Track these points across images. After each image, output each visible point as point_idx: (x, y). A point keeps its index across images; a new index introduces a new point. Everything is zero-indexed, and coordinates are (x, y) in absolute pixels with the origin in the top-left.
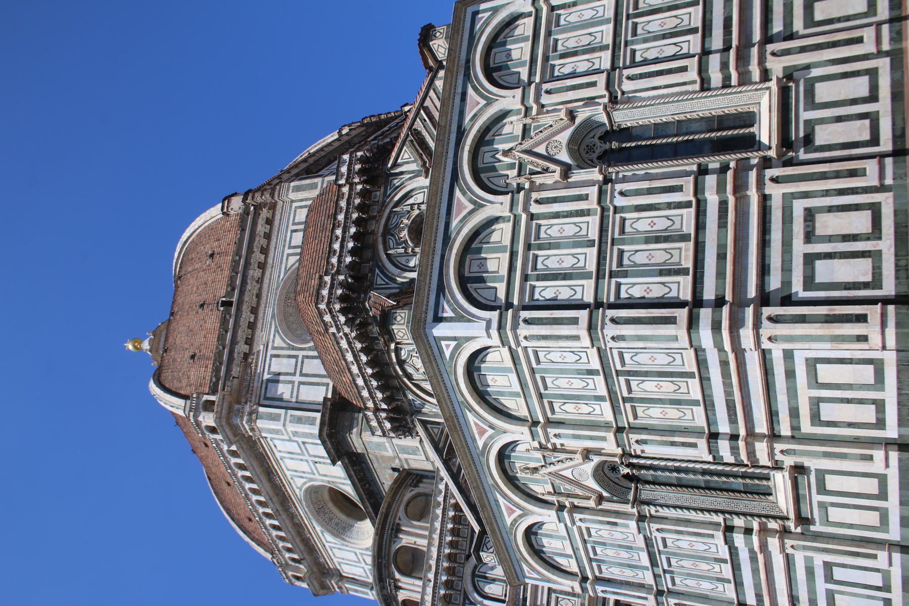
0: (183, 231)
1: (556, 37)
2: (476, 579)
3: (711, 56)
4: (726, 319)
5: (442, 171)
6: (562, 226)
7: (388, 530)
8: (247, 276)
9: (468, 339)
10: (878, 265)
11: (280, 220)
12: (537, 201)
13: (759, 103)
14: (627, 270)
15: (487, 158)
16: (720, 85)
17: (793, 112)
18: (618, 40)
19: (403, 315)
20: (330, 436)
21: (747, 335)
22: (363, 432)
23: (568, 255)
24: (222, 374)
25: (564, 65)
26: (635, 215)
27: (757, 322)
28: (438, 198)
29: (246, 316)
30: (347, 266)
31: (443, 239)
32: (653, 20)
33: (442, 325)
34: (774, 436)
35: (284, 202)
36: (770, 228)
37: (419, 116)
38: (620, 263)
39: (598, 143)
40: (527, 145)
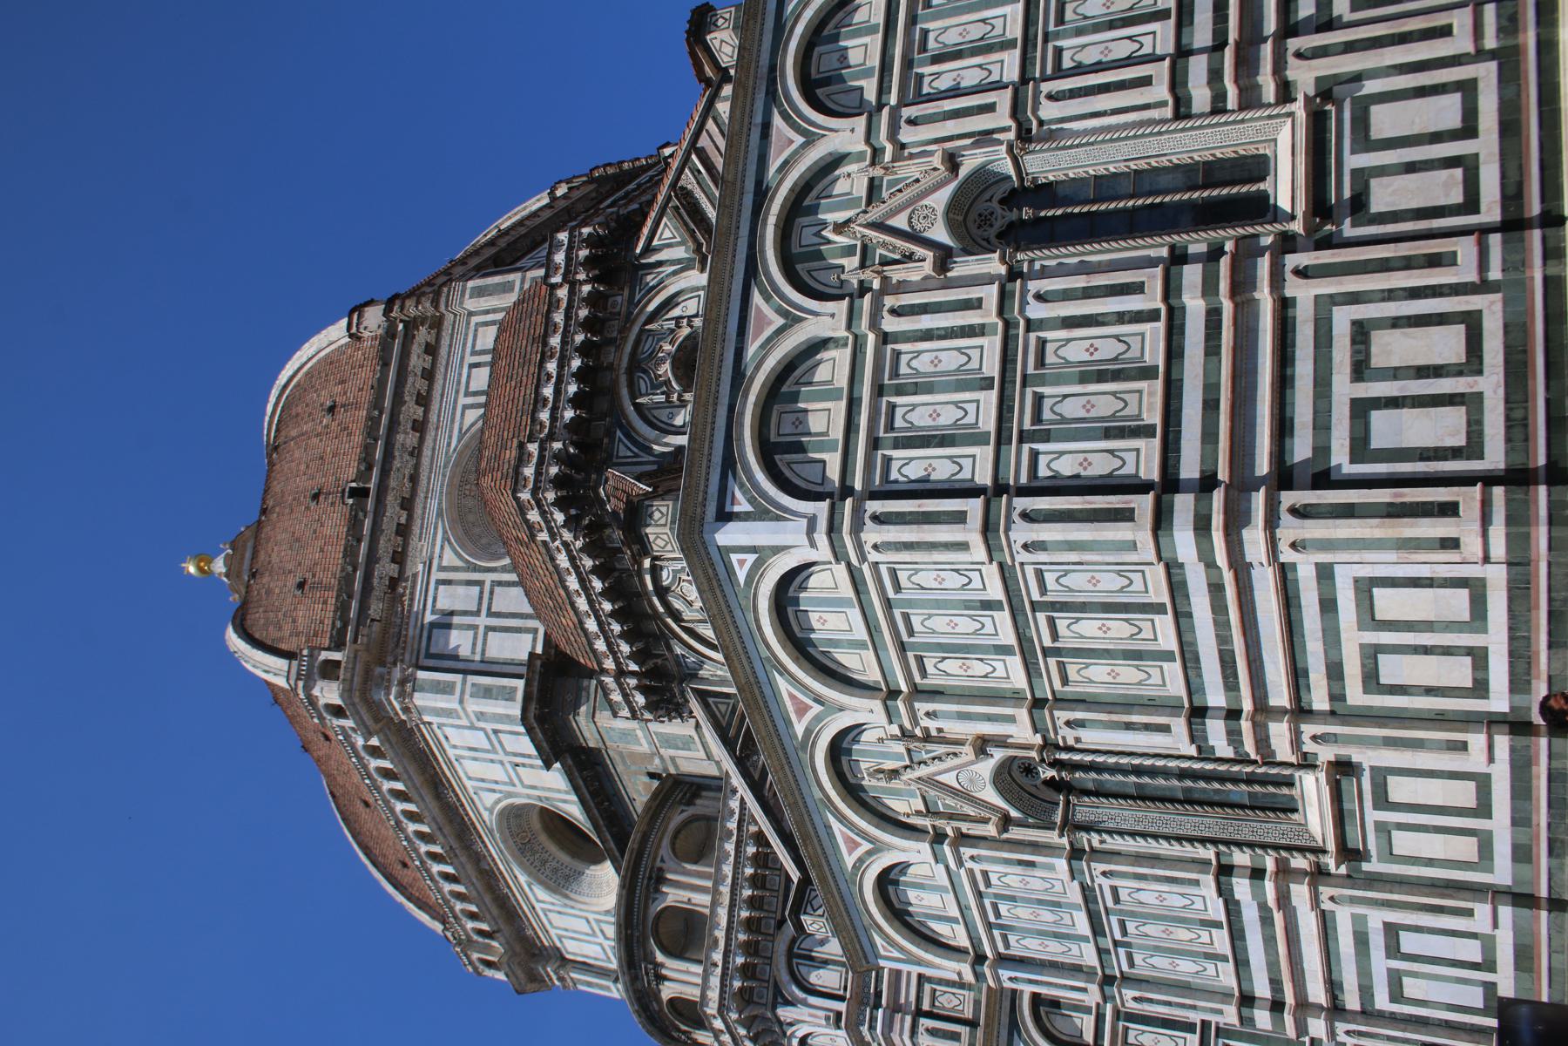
0: (282, 367)
1: (925, 26)
2: (795, 960)
3: (1192, 59)
4: (1219, 513)
5: (729, 260)
7: (643, 879)
8: (394, 445)
9: (777, 550)
11: (450, 346)
13: (1275, 140)
14: (1049, 430)
15: (808, 237)
16: (1208, 109)
17: (1333, 156)
19: (664, 510)
20: (541, 719)
21: (1254, 540)
22: (597, 712)
23: (947, 403)
25: (938, 74)
26: (1063, 334)
27: (1272, 516)
28: (723, 307)
29: (393, 513)
30: (566, 426)
31: (733, 378)
33: (731, 525)
34: (1300, 712)
35: (456, 315)
37: (690, 164)
38: (1037, 417)
40: (875, 213)
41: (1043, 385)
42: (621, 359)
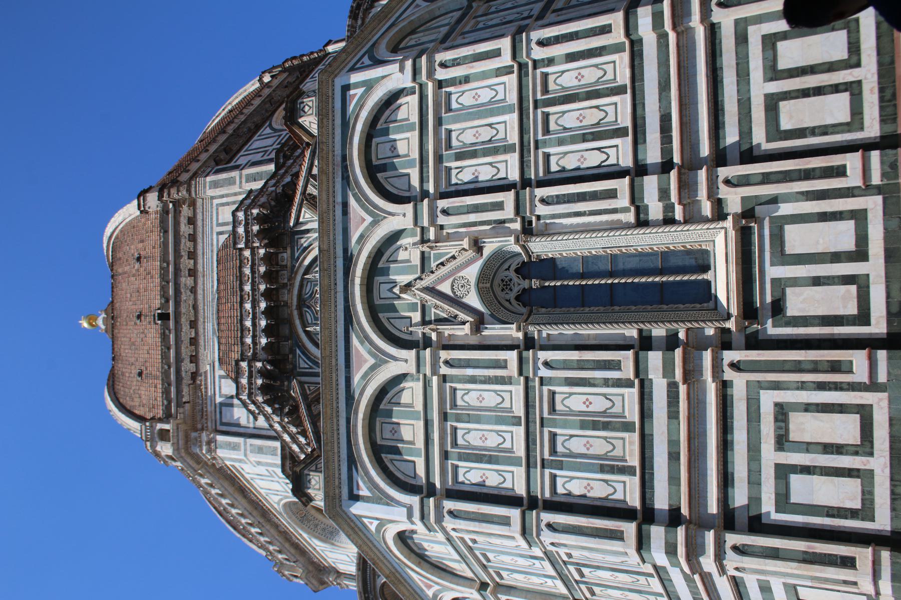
1: (449, 127)
4: (682, 545)
5: (333, 310)
6: (481, 392)
12: (447, 363)
14: (562, 461)
16: (661, 217)
17: (757, 267)
18: (526, 137)
21: (708, 563)
23: (491, 431)
25: (461, 168)
26: (566, 389)
27: (720, 551)
28: (333, 345)
30: (263, 349)
38: (553, 451)
39: (515, 280)
40: (428, 281)
41: (555, 427)
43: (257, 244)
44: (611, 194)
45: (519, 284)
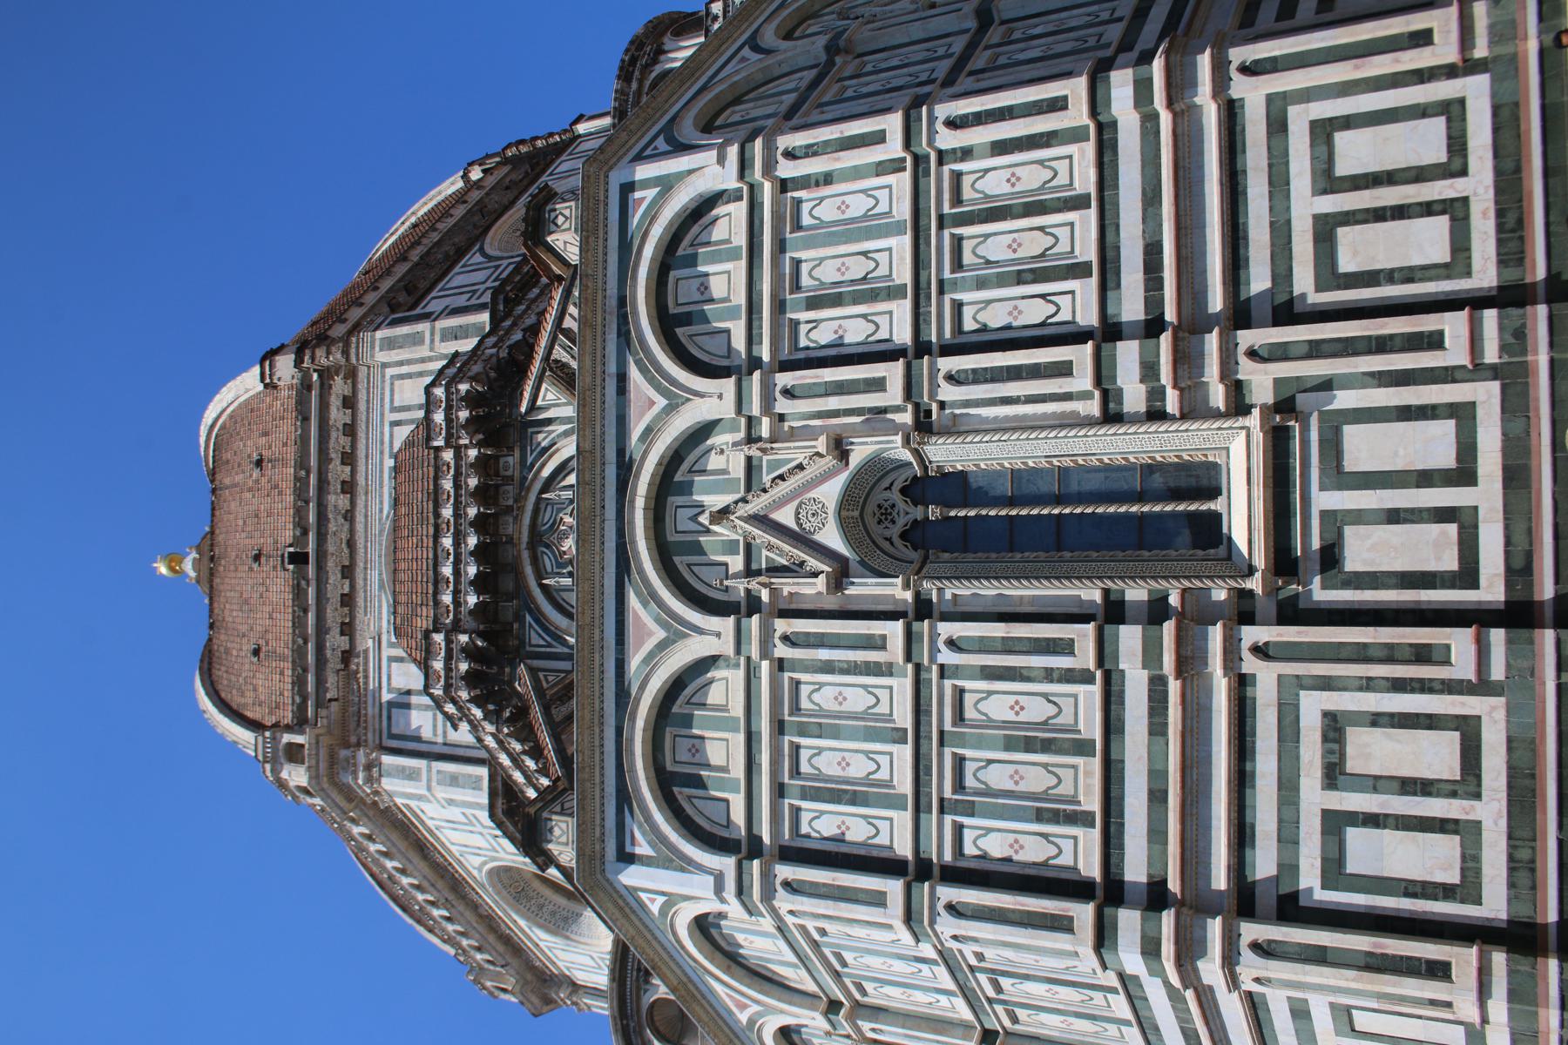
1: (796, 255)
3: (1121, 346)
4: (1169, 940)
5: (597, 549)
8: (326, 507)
10: (1473, 852)
11: (368, 401)
12: (786, 639)
14: (973, 802)
15: (683, 519)
16: (1143, 409)
17: (1298, 492)
19: (564, 826)
21: (1211, 970)
23: (857, 751)
24: (311, 687)
25: (816, 323)
27: (1230, 950)
28: (597, 607)
29: (336, 585)
30: (471, 612)
31: (617, 695)
32: (995, 234)
33: (633, 868)
35: (369, 367)
36: (1254, 748)
37: (559, 342)
38: (959, 786)
39: (901, 505)
40: (756, 505)
41: (963, 747)
42: (520, 533)
43: (465, 441)
44: (1064, 369)
45: (907, 513)
